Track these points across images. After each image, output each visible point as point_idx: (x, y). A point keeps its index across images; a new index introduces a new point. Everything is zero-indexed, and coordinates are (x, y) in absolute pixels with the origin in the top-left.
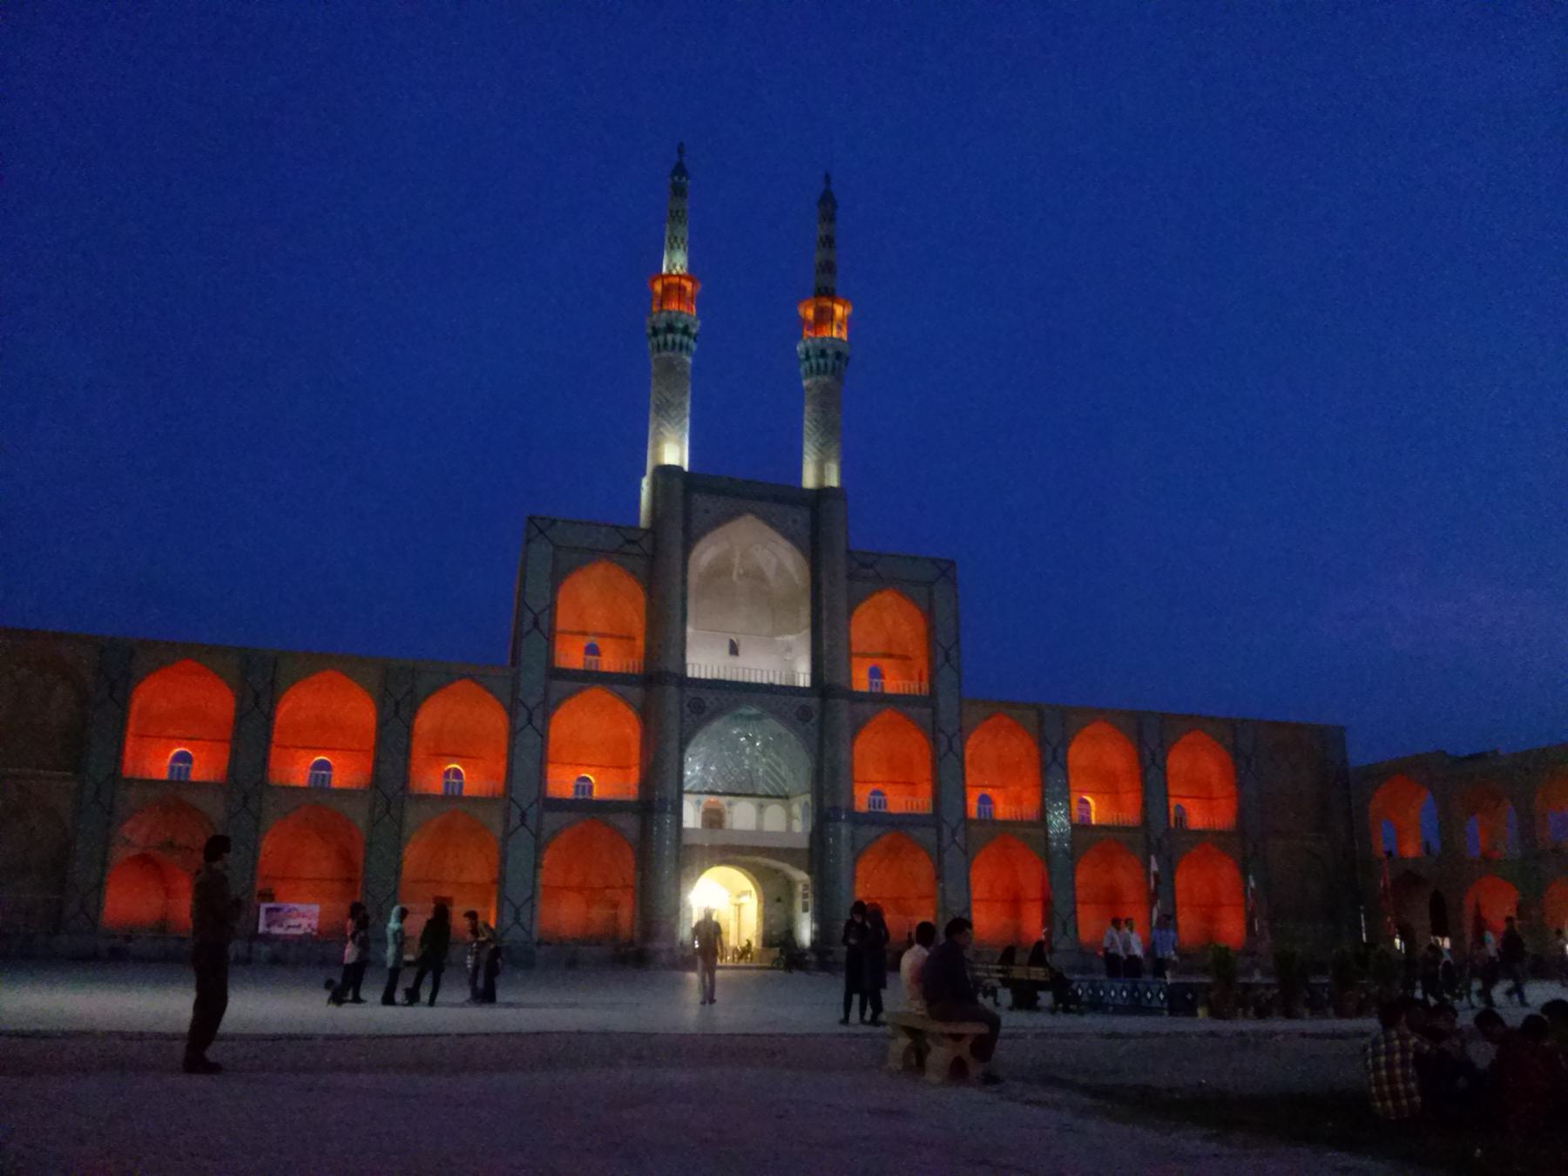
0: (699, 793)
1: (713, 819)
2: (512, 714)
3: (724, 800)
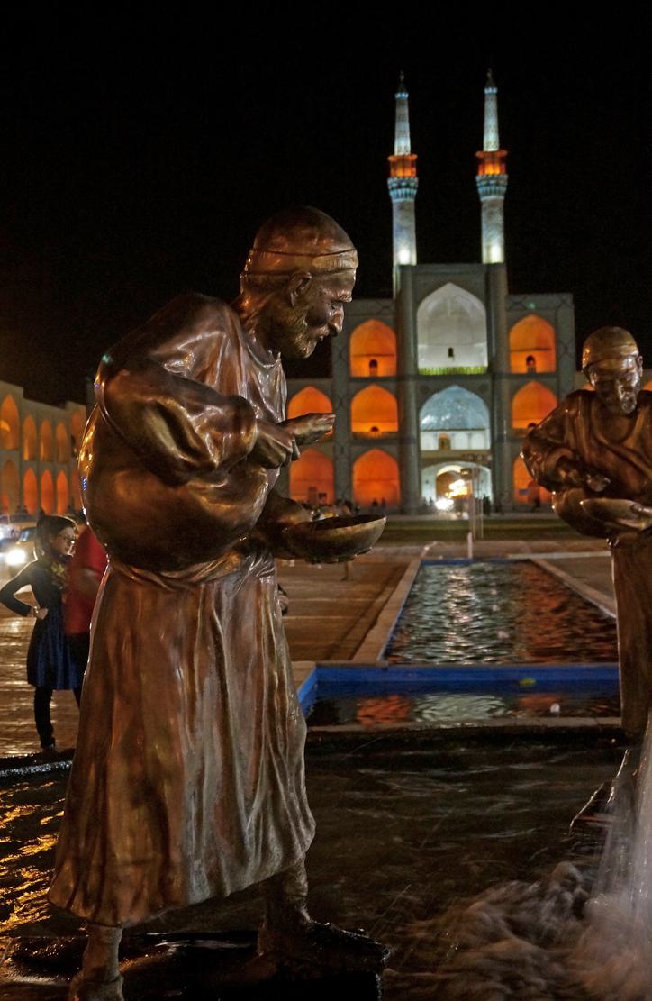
0: (437, 430)
1: (444, 443)
3: (449, 433)
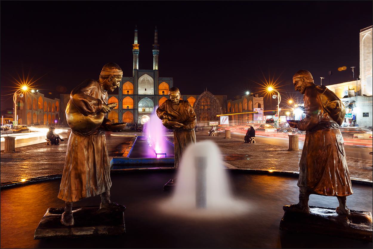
2: (118, 100)
3: (145, 108)
